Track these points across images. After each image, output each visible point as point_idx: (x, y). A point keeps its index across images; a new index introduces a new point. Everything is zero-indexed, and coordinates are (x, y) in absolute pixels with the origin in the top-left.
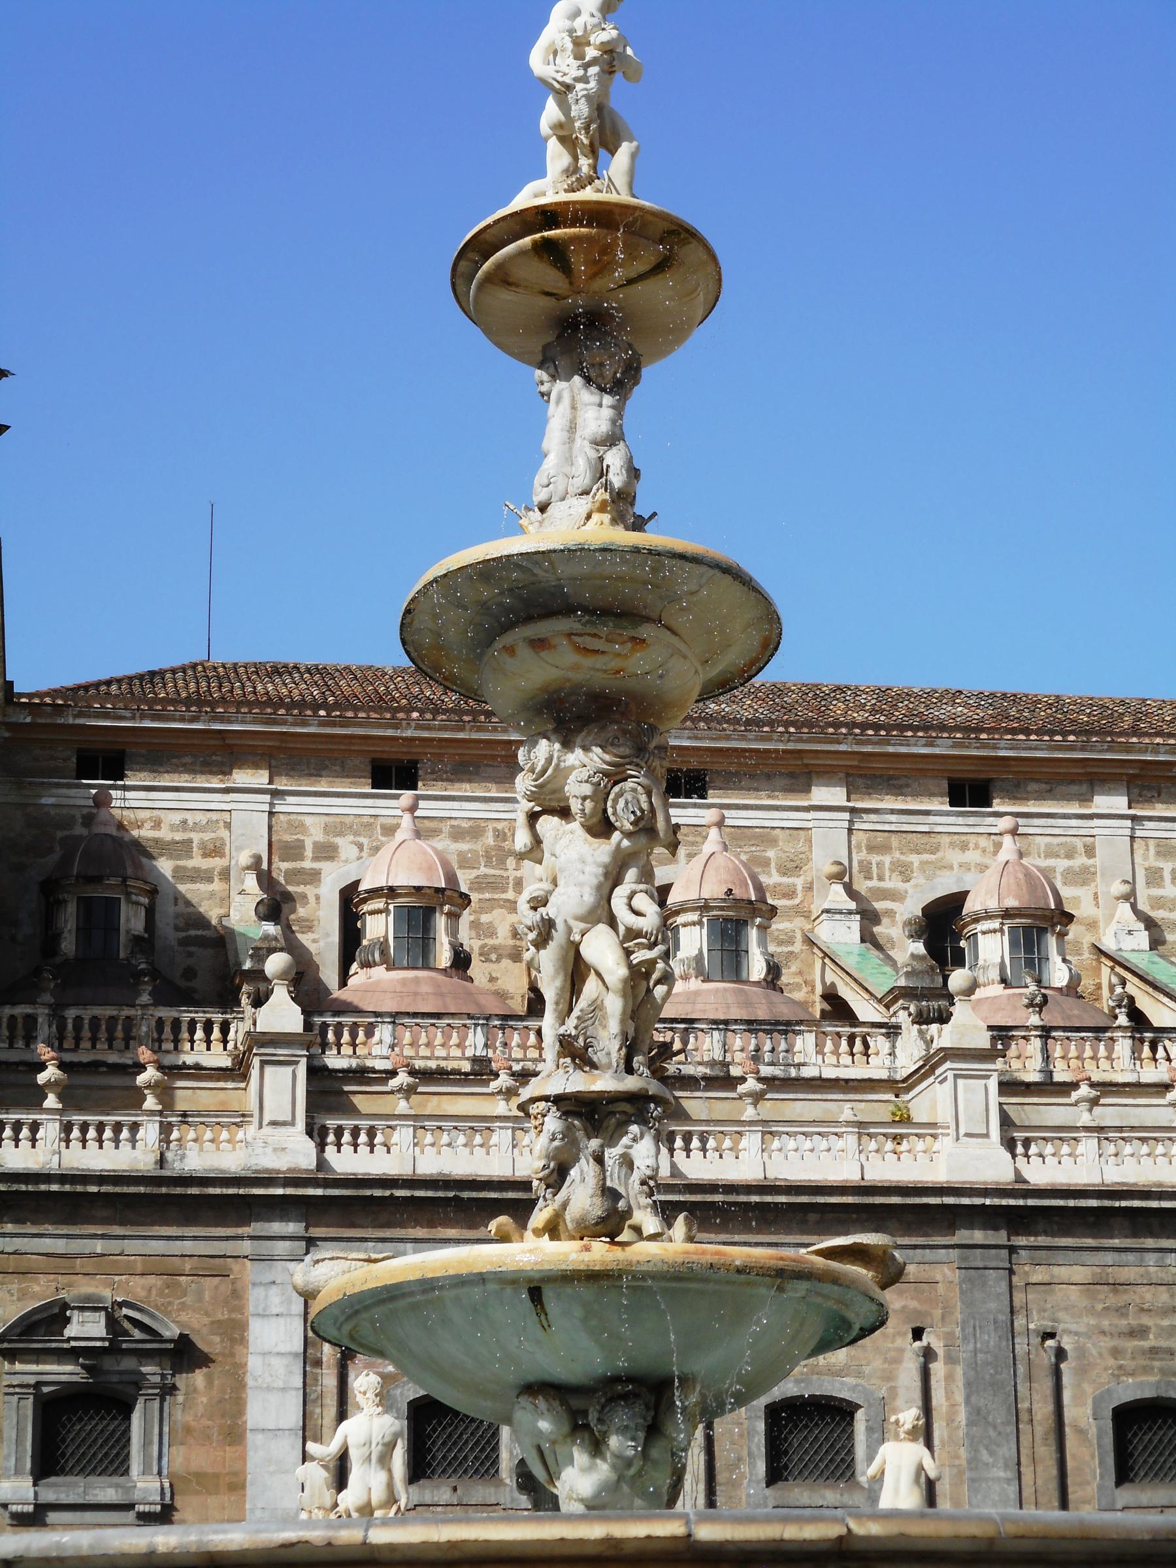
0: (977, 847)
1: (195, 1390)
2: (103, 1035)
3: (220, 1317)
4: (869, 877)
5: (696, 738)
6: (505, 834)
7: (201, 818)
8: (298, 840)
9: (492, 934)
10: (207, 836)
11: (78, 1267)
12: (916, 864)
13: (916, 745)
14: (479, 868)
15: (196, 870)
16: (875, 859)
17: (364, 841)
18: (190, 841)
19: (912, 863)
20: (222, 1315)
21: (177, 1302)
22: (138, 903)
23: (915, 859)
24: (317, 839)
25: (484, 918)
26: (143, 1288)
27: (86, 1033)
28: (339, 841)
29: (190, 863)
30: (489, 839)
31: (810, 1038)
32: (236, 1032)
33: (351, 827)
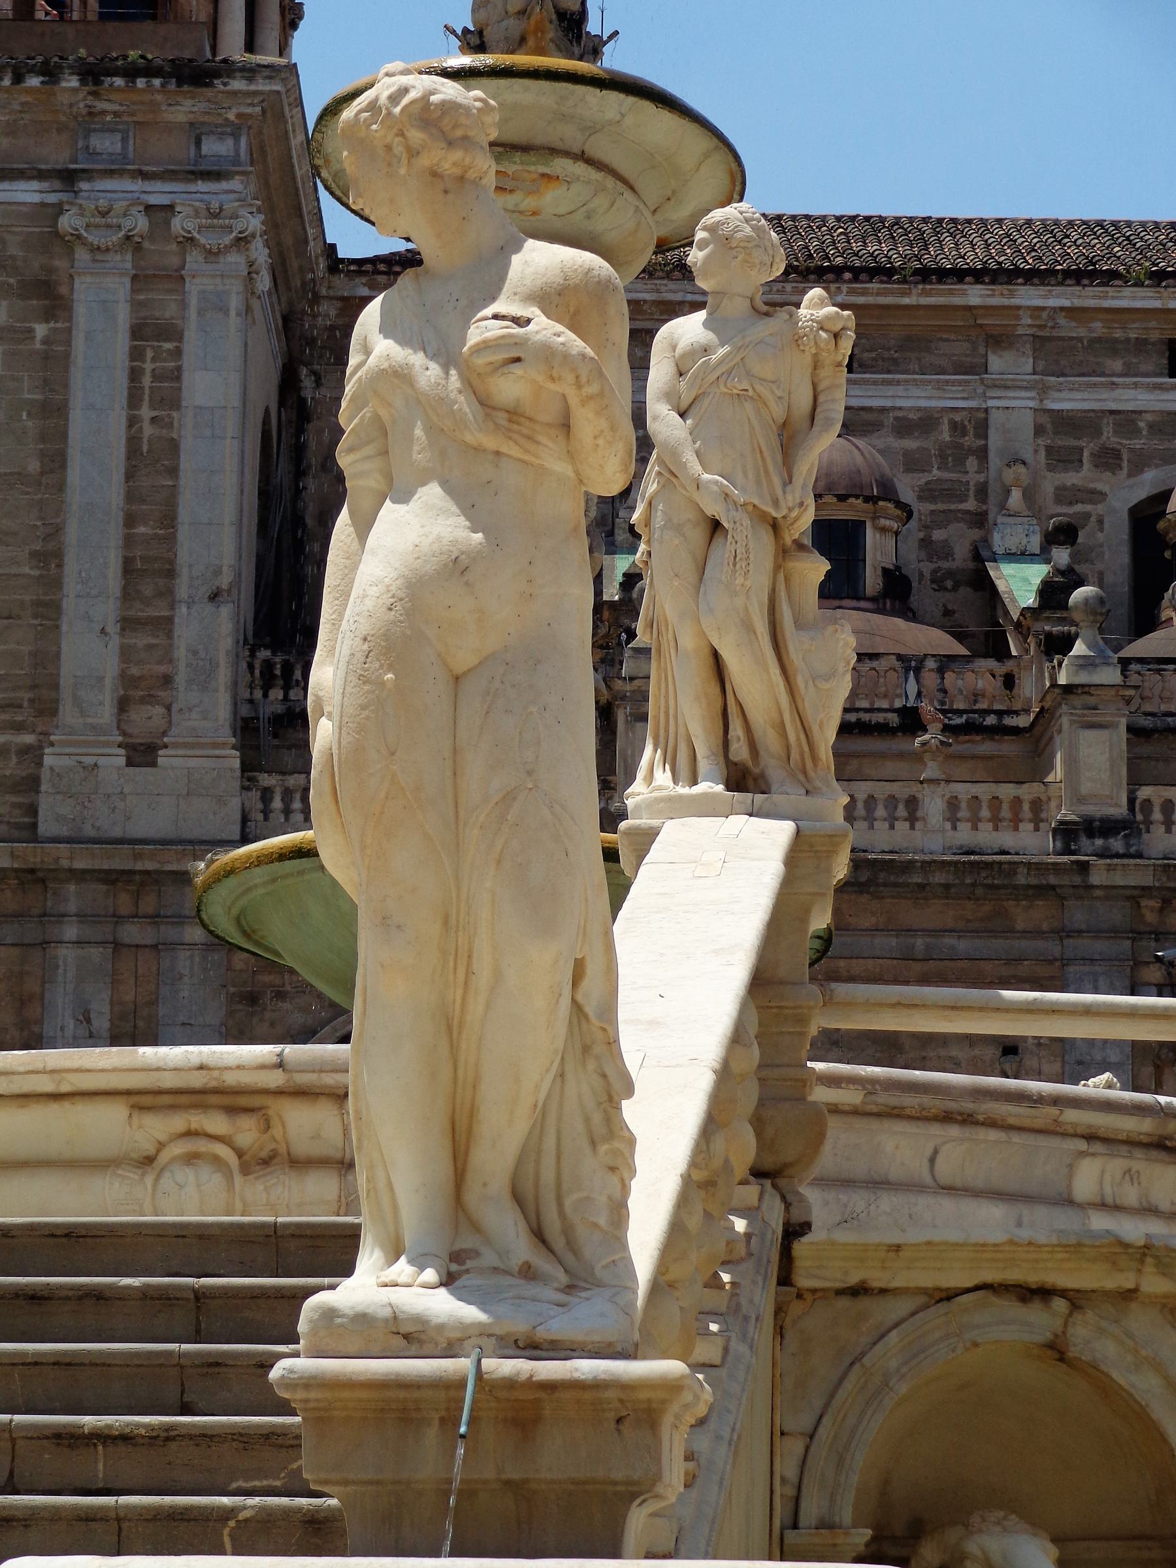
6: (964, 427)
9: (948, 555)
14: (930, 472)
25: (938, 535)
30: (946, 436)
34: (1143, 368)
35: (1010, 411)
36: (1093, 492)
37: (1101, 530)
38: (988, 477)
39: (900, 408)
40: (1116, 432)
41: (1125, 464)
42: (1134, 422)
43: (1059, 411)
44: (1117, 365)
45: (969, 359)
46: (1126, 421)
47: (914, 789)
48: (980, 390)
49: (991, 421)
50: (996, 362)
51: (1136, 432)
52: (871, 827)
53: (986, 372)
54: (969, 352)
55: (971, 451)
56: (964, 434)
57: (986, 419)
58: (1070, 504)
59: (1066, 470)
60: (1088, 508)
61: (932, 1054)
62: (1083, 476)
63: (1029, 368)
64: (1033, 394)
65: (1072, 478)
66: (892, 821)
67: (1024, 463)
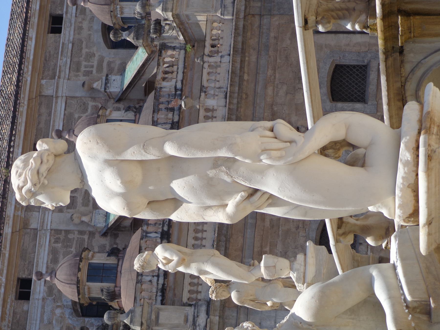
0: (81, 22)
4: (91, 72)
5: (18, 146)
6: (57, 238)
12: (87, 50)
13: (31, 46)
16: (83, 69)
19: (86, 52)
23: (84, 51)
30: (60, 245)
31: (164, 84)
35: (52, 221)
38: (76, 230)
39: (47, 261)
45: (31, 235)
48: (43, 232)
49: (55, 228)
50: (34, 225)
52: (205, 239)
53: (37, 229)
54: (29, 236)
56: (59, 238)
57: (55, 230)
63: (37, 213)
66: (203, 231)
67: (72, 215)
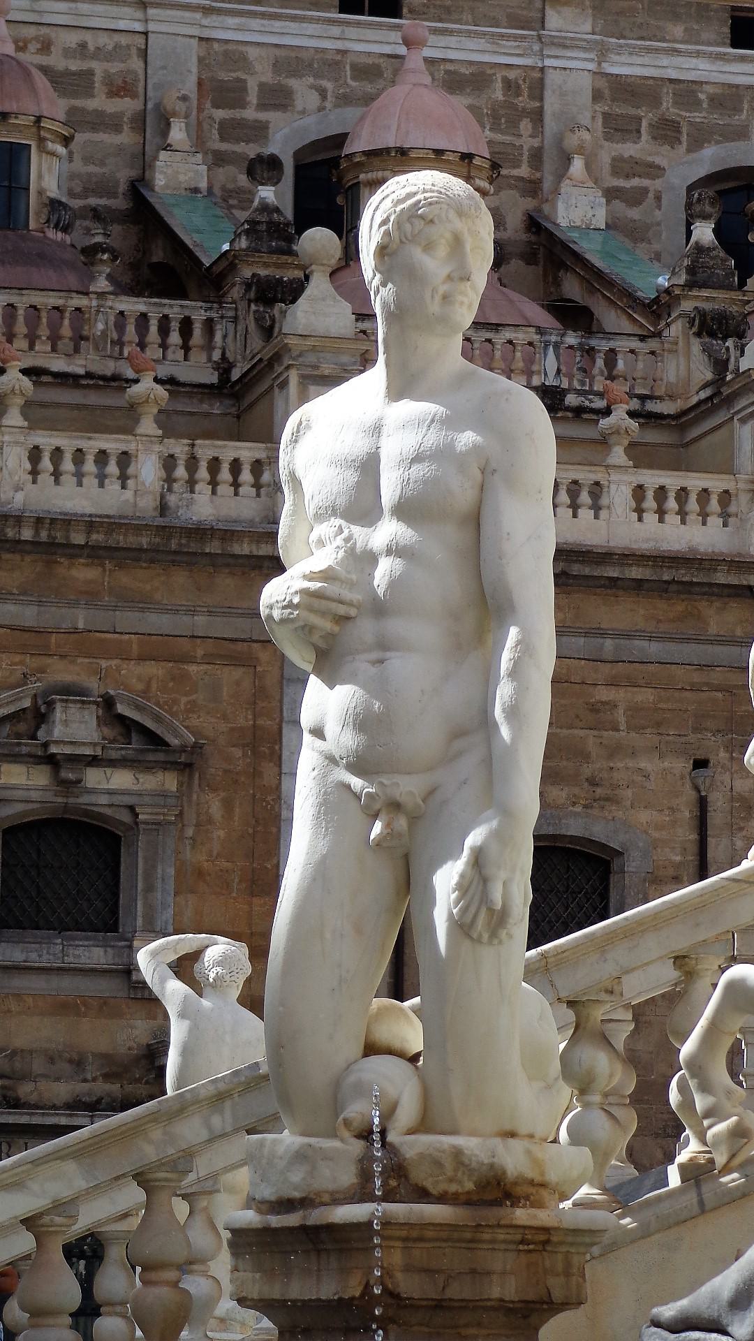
1: (210, 821)
2: (44, 332)
3: (241, 722)
6: (518, 87)
7: (104, 40)
8: (238, 80)
10: (115, 67)
11: (53, 646)
15: (100, 114)
17: (329, 85)
18: (91, 73)
20: (243, 720)
21: (184, 700)
22: (53, 154)
24: (264, 79)
26: (139, 679)
27: (21, 328)
28: (293, 83)
29: (92, 104)
30: (499, 95)
32: (225, 337)
33: (310, 65)
34: (705, 36)
35: (568, 72)
36: (651, 165)
37: (659, 207)
38: (543, 141)
39: (451, 61)
40: (675, 103)
41: (684, 138)
42: (694, 92)
43: (617, 75)
44: (678, 30)
45: (525, 13)
46: (686, 92)
47: (599, 476)
48: (536, 47)
49: (548, 81)
50: (555, 20)
51: (695, 104)
54: (523, 5)
55: (525, 113)
58: (627, 177)
59: (624, 141)
60: (646, 182)
61: (620, 765)
62: (640, 148)
63: (588, 27)
64: (592, 56)
65: (629, 149)
